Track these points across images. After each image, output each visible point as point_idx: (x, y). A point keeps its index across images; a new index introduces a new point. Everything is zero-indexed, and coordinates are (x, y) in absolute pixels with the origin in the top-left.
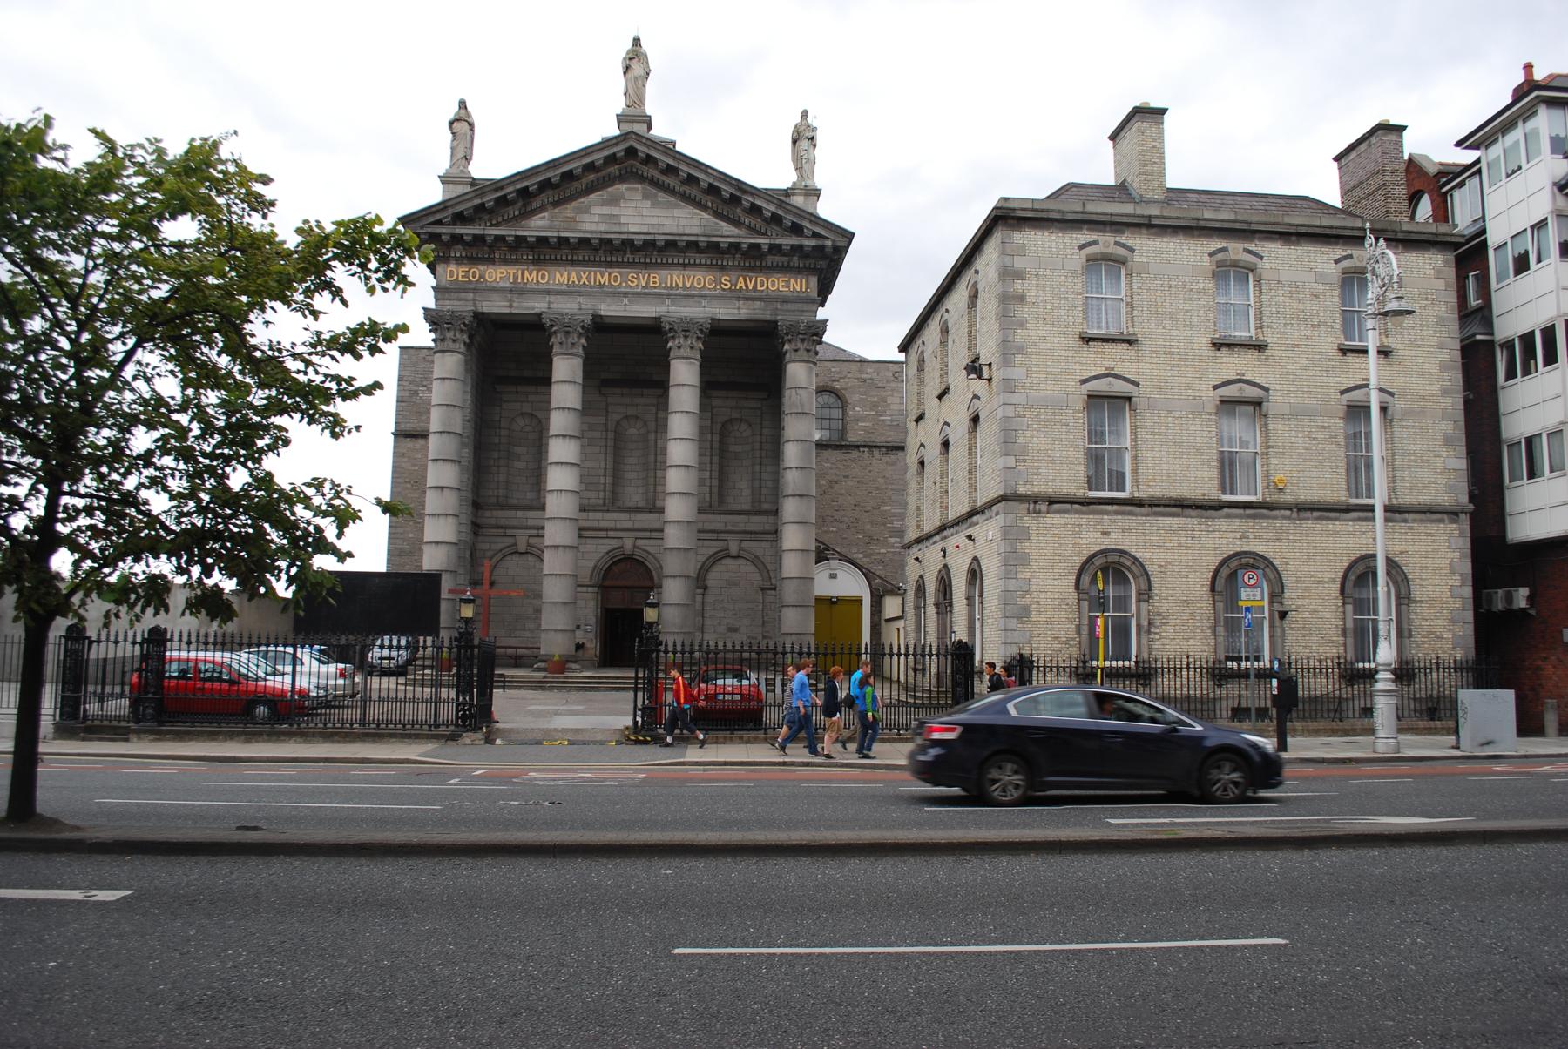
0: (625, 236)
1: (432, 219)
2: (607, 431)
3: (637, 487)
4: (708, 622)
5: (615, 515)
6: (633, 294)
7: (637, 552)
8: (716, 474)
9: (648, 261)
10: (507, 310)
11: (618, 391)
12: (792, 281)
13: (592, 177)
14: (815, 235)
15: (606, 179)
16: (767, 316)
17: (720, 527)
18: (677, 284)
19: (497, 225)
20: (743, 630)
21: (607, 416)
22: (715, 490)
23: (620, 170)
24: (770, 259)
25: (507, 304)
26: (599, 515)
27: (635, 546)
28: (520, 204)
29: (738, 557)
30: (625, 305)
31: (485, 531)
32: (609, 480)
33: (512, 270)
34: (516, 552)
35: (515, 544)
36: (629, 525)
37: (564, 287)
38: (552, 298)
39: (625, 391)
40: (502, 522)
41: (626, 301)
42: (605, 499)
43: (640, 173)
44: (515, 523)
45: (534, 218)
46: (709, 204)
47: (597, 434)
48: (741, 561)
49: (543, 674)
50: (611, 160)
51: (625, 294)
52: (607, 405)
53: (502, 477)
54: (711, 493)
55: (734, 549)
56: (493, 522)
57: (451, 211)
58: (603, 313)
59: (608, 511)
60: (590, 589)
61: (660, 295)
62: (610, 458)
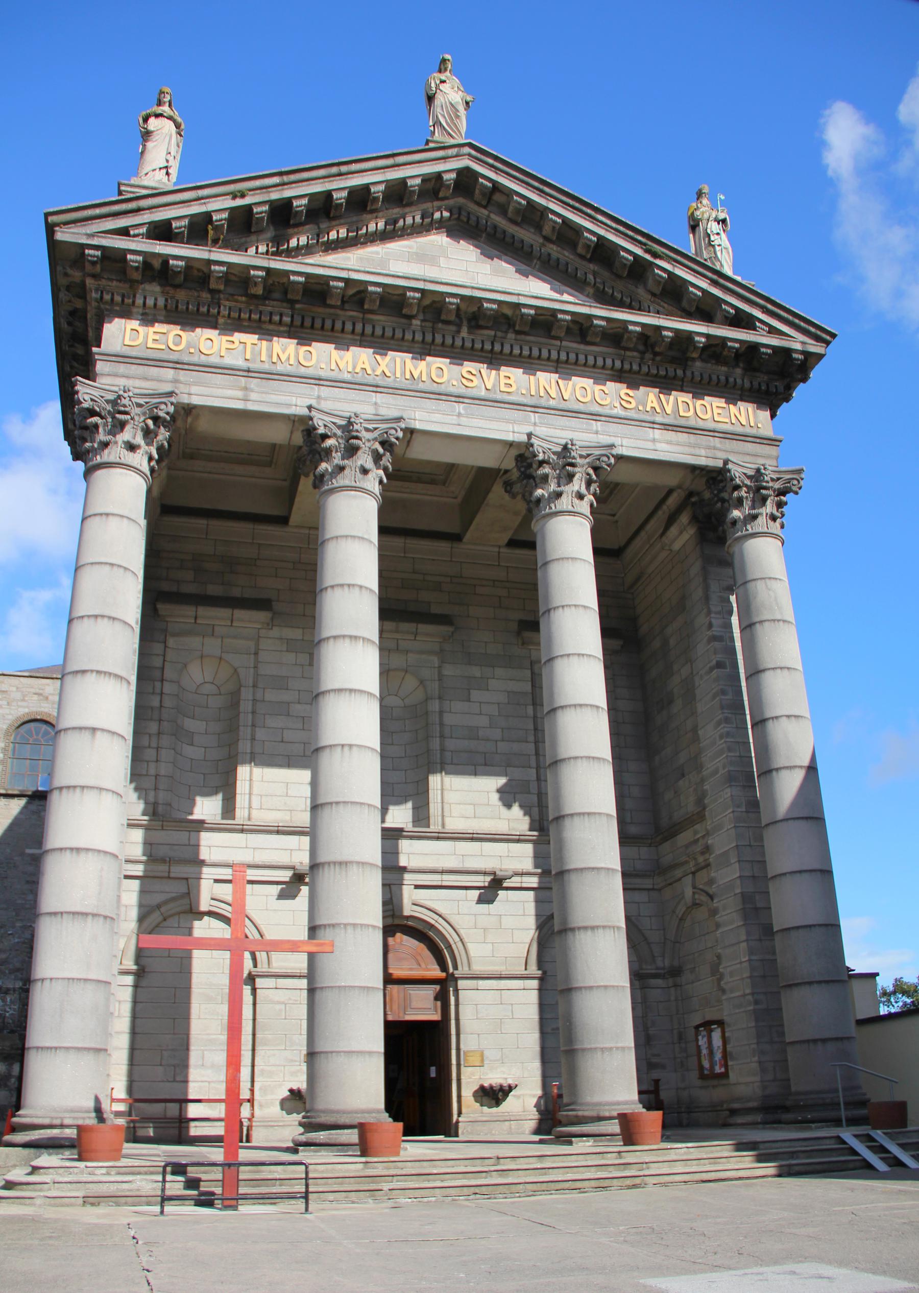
9: (497, 348)
25: (240, 394)
30: (459, 415)
37: (347, 377)
38: (325, 391)
41: (460, 408)
46: (590, 277)
51: (459, 398)
57: (147, 217)
58: (418, 426)
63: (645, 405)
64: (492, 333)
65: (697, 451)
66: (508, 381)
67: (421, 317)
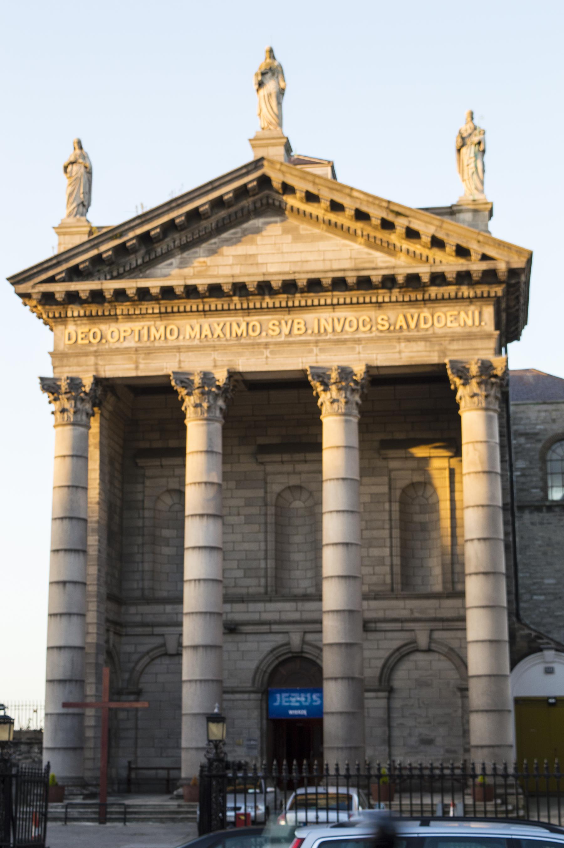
0: (261, 279)
1: (44, 276)
2: (266, 505)
3: (306, 570)
4: (396, 733)
5: (279, 606)
6: (276, 344)
7: (307, 648)
8: (397, 551)
10: (133, 374)
11: (277, 458)
12: (463, 314)
13: (223, 213)
14: (485, 257)
15: (239, 214)
16: (434, 358)
17: (405, 614)
18: (325, 330)
19: (119, 277)
20: (439, 741)
21: (265, 488)
22: (397, 570)
23: (254, 203)
24: (433, 291)
26: (260, 606)
27: (304, 642)
28: (142, 252)
29: (429, 650)
31: (130, 631)
32: (271, 563)
33: (137, 325)
34: (166, 654)
35: (164, 645)
36: (296, 616)
37: (196, 342)
38: (183, 356)
39: (286, 457)
40: (149, 619)
41: (267, 353)
42: (266, 587)
43: (277, 203)
44: (164, 619)
45: (160, 266)
47: (255, 510)
48: (435, 656)
49: (175, 803)
50: (242, 192)
51: (267, 345)
52: (266, 474)
53: (147, 566)
54: (392, 574)
55: (423, 640)
56: (138, 619)
58: (241, 369)
59: (270, 601)
60: (253, 696)
61: (306, 343)
62: (271, 537)
63: (395, 325)
64: (285, 296)
65: (432, 354)
66: (299, 326)
67: (238, 293)
